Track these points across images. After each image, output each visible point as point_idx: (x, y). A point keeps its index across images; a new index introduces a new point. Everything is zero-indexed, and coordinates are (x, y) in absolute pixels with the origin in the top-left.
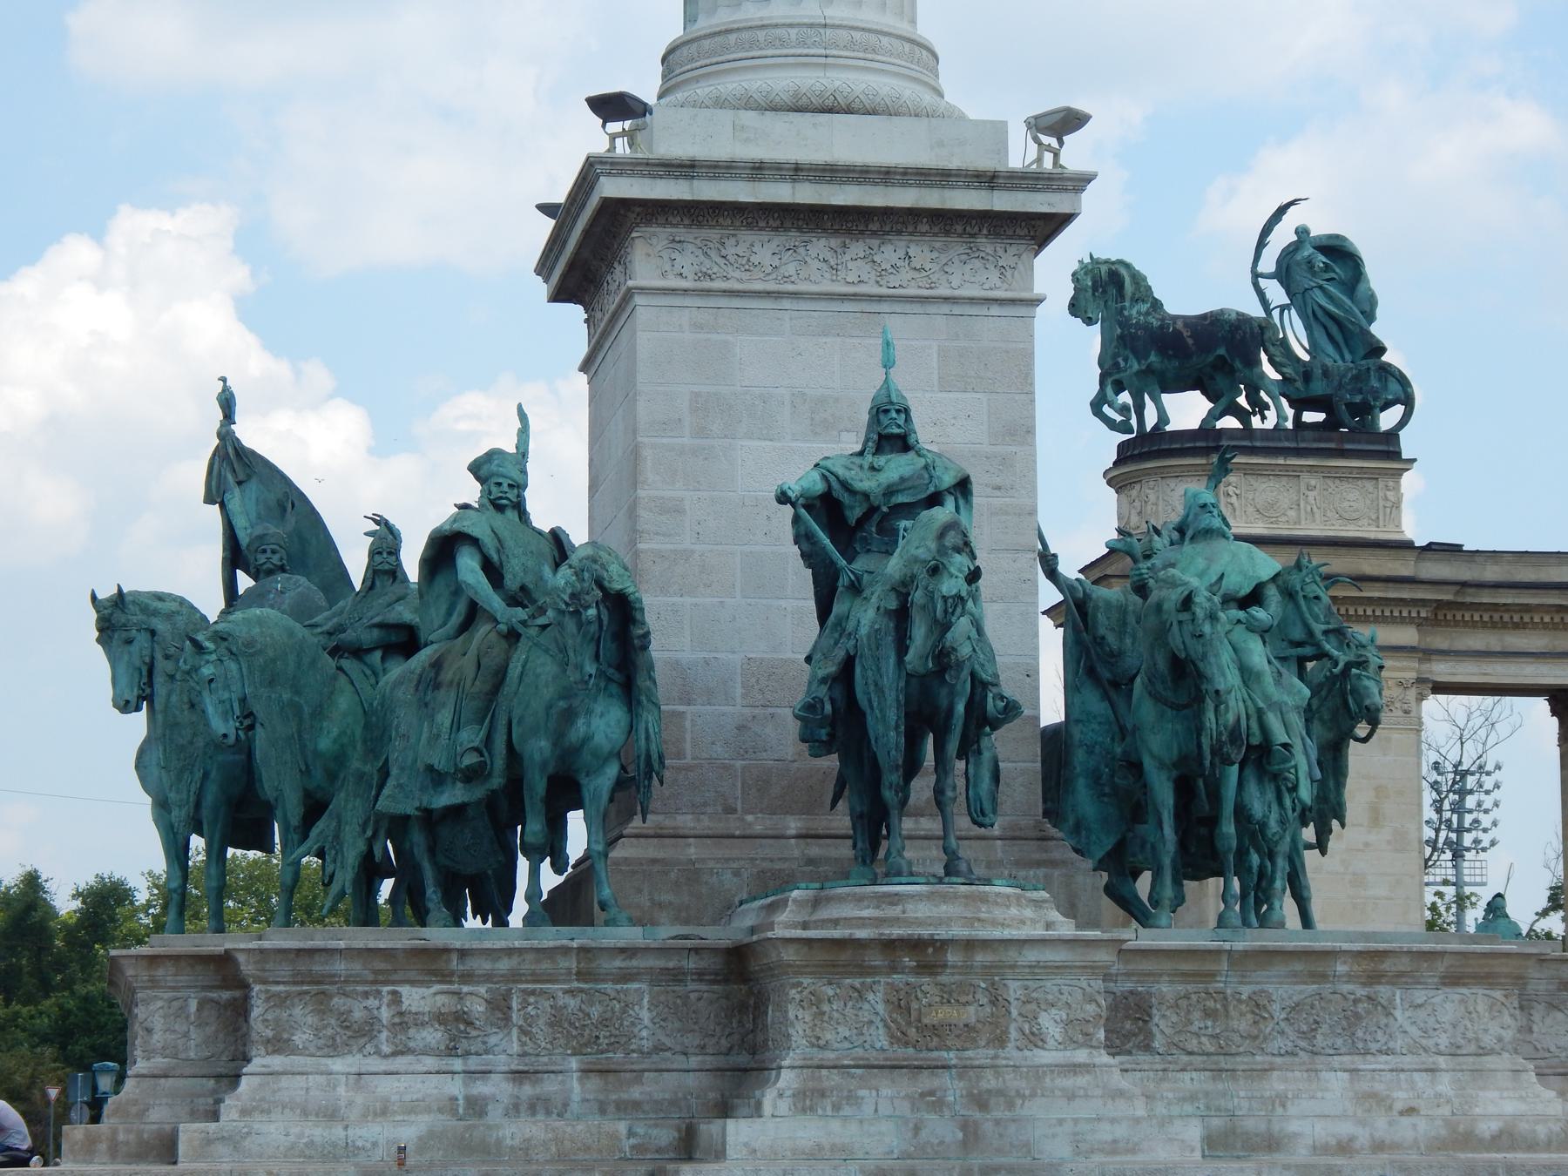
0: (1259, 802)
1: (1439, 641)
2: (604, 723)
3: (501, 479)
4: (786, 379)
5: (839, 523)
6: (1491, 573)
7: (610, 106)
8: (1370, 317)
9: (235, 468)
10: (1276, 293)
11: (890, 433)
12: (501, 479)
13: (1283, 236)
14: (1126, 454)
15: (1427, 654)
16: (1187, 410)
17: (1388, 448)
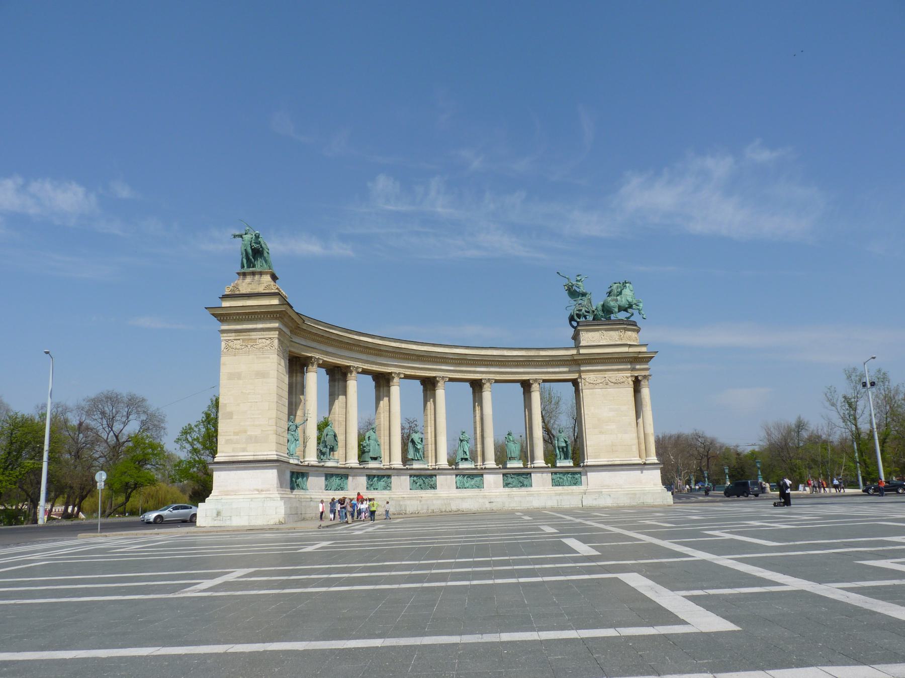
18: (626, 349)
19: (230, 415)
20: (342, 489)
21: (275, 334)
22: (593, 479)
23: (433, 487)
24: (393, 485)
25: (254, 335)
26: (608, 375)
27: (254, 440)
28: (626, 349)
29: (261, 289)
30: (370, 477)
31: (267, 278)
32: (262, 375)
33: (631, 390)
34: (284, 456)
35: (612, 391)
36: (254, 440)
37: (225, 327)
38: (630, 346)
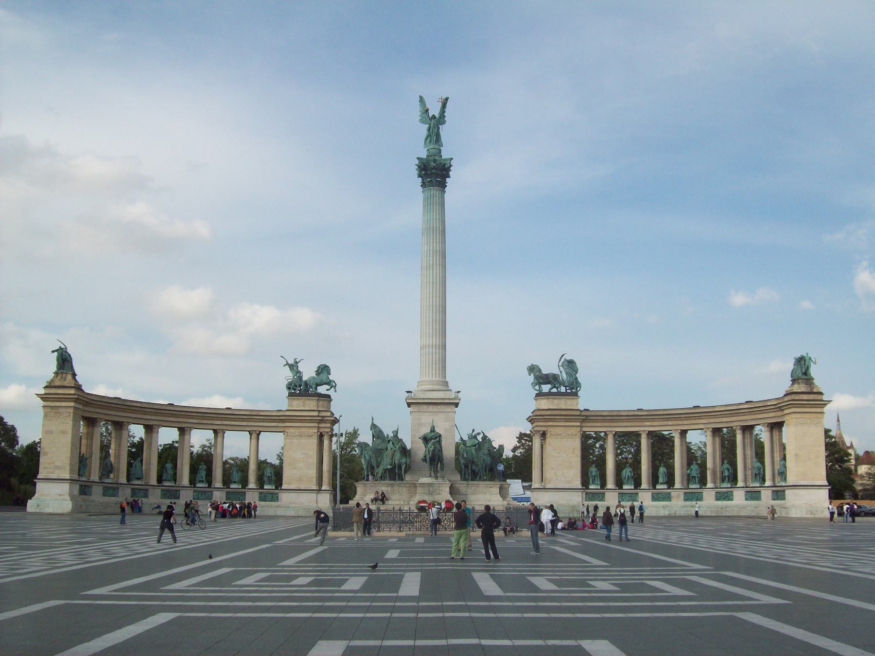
0: (474, 468)
1: (584, 424)
2: (404, 460)
3: (396, 433)
4: (428, 420)
5: (426, 440)
6: (593, 414)
7: (408, 392)
8: (577, 372)
9: (374, 426)
10: (561, 368)
11: (433, 430)
12: (396, 433)
13: (563, 360)
14: (537, 395)
15: (581, 427)
16: (546, 388)
17: (576, 394)
18: (316, 414)
19: (46, 454)
20: (114, 496)
21: (72, 410)
22: (285, 497)
23: (178, 498)
24: (150, 495)
25: (61, 410)
26: (303, 430)
27: (58, 468)
28: (316, 414)
29: (66, 384)
30: (132, 489)
31: (69, 377)
32: (64, 432)
33: (314, 441)
34: (76, 477)
35: (304, 440)
36: (58, 468)
37: (46, 404)
38: (319, 411)
